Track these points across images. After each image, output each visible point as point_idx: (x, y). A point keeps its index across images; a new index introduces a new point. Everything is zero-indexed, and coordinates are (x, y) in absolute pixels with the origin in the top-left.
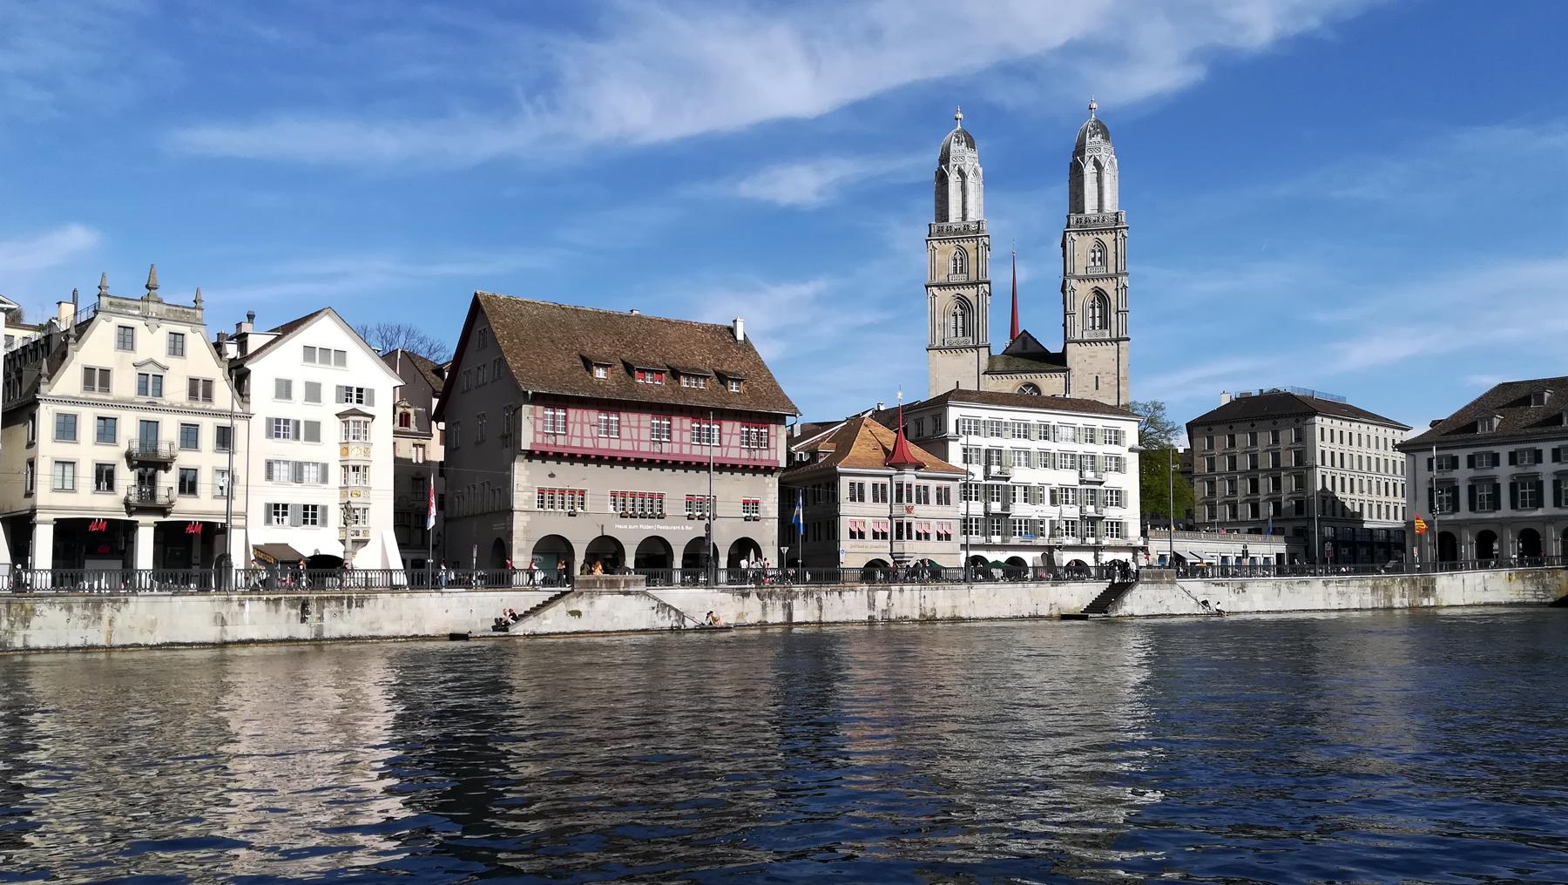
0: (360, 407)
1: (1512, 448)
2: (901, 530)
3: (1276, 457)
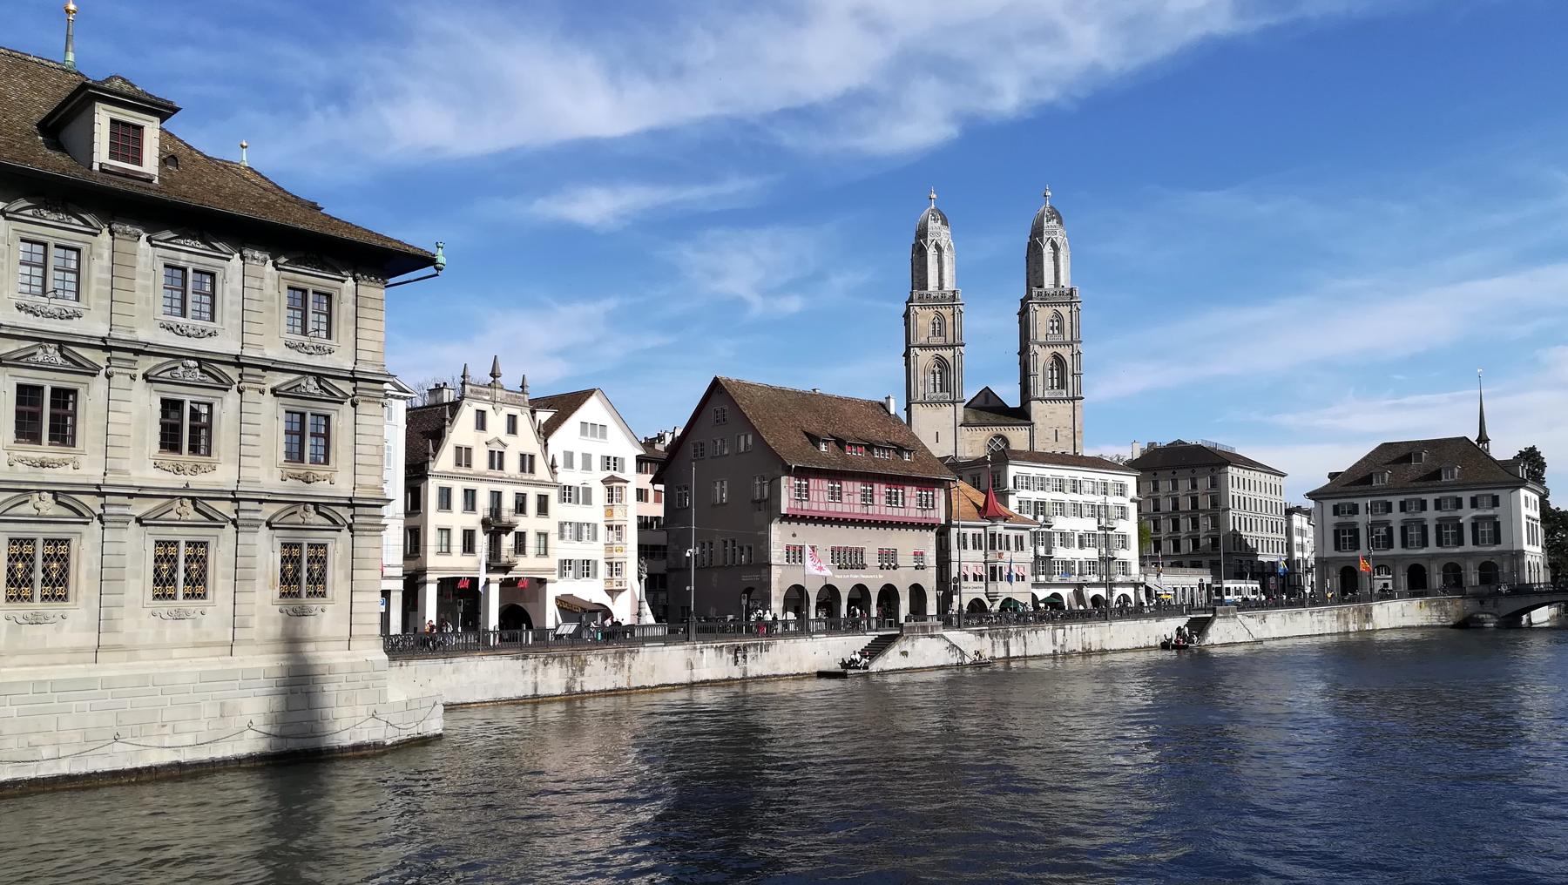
0: (617, 474)
1: (1402, 498)
2: (994, 574)
3: (1195, 500)
